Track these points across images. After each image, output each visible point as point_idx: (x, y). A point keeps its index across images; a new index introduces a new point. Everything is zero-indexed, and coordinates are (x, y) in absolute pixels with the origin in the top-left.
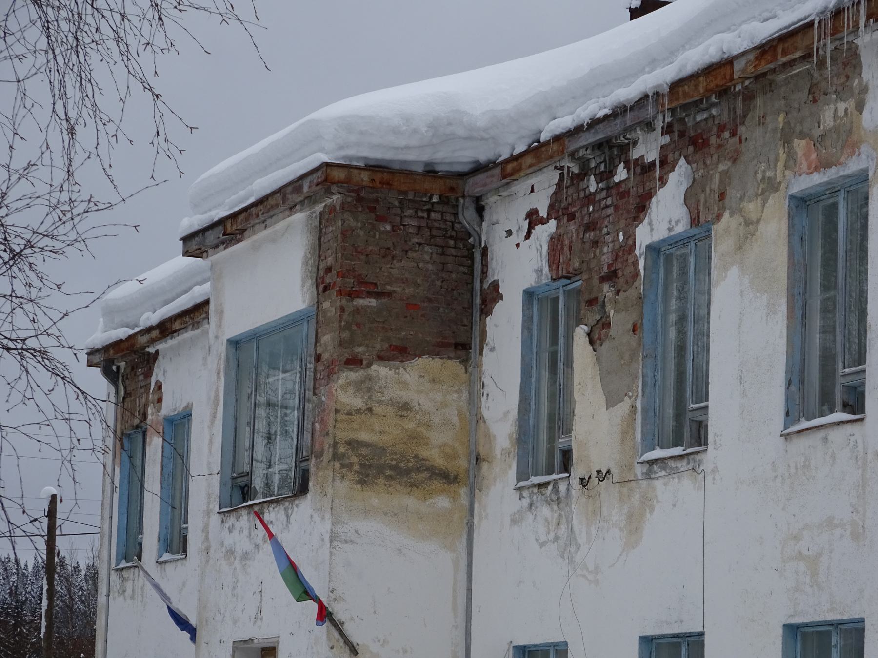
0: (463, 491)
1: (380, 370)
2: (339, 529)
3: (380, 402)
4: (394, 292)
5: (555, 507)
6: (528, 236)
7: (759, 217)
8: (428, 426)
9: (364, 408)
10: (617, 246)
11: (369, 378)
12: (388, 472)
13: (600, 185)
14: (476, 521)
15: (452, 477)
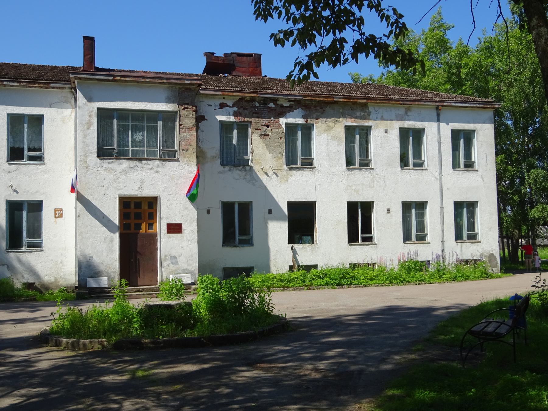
5: (244, 172)
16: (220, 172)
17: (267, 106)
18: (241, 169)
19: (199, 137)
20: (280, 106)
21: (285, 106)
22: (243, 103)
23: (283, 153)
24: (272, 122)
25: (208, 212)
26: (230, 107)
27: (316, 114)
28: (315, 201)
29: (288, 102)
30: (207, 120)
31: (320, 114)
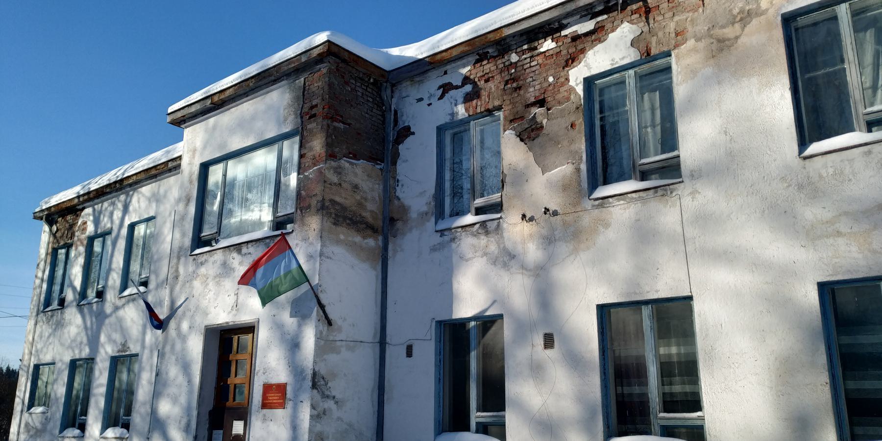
0: (380, 238)
1: (344, 163)
2: (325, 250)
3: (345, 181)
4: (351, 124)
5: (483, 237)
6: (441, 98)
7: (738, 34)
8: (366, 199)
9: (338, 183)
10: (545, 85)
11: (340, 167)
12: (348, 221)
13: (523, 57)
14: (390, 253)
15: (375, 229)
16: (434, 249)
17: (537, 52)
18: (477, 230)
19: (397, 177)
20: (570, 40)
21: (587, 34)
22: (485, 67)
23: (581, 162)
24: (551, 88)
25: (409, 352)
26: (457, 87)
27: (676, 18)
28: (686, 293)
29: (591, 19)
30: (413, 133)
31: (687, 14)
